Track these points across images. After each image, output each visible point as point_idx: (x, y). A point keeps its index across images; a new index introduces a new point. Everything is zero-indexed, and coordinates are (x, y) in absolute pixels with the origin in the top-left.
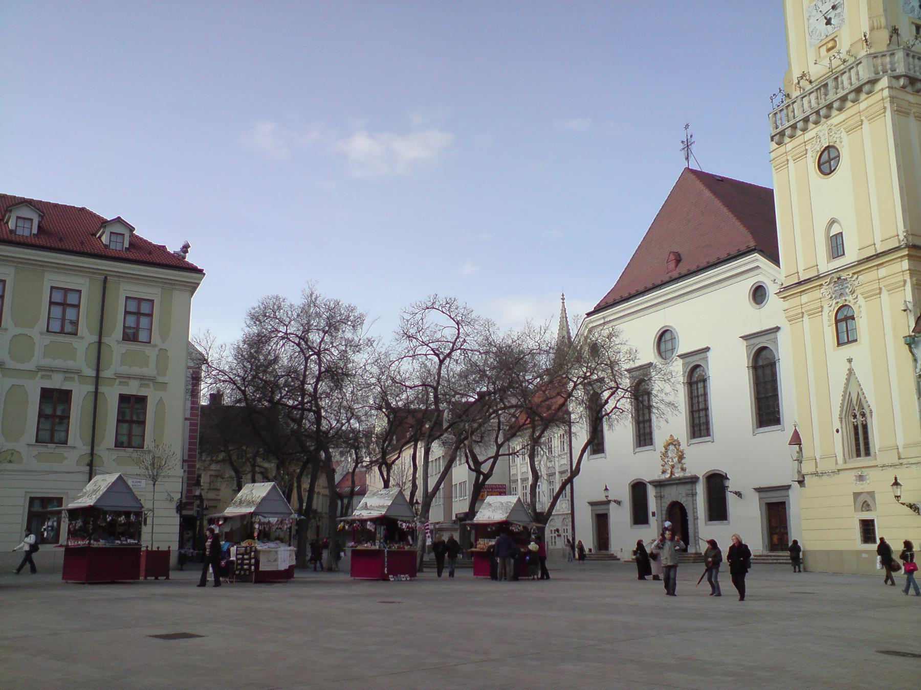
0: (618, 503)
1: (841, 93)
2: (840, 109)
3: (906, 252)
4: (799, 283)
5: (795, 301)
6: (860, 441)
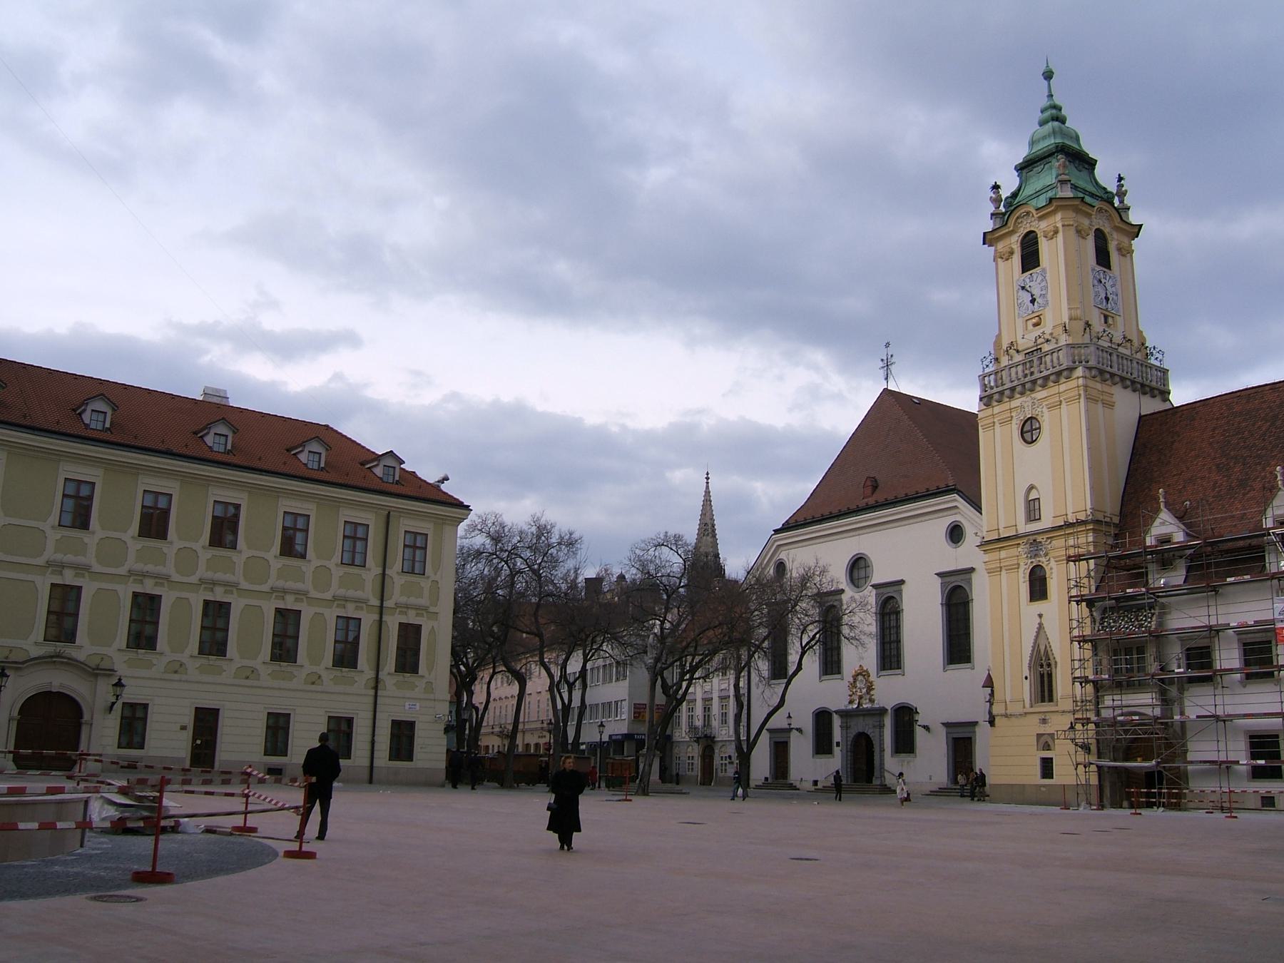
0: (799, 730)
1: (1045, 373)
2: (1044, 386)
4: (999, 540)
5: (994, 555)
6: (1044, 688)
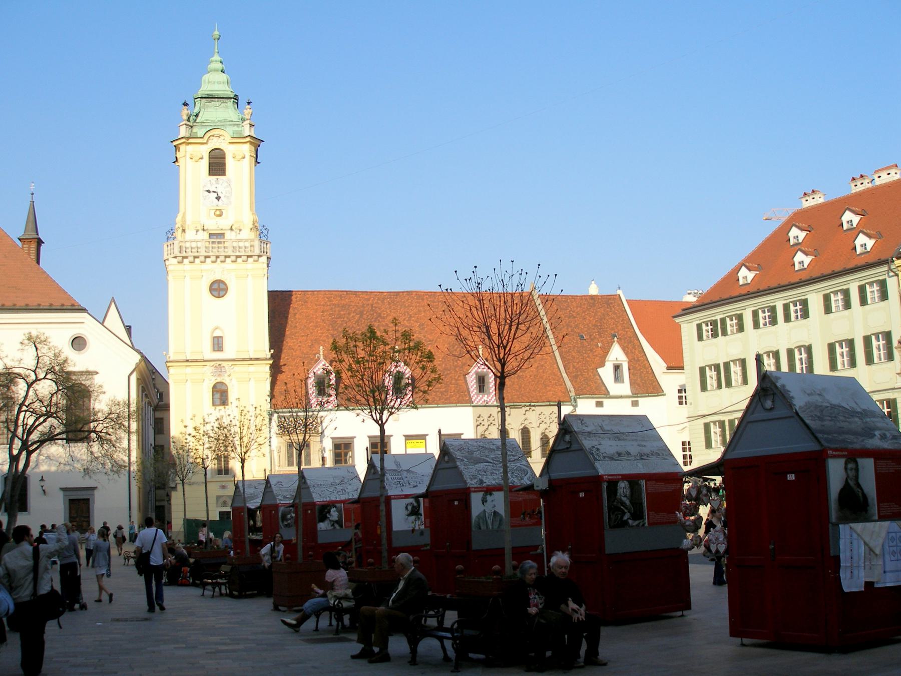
3: (271, 362)
